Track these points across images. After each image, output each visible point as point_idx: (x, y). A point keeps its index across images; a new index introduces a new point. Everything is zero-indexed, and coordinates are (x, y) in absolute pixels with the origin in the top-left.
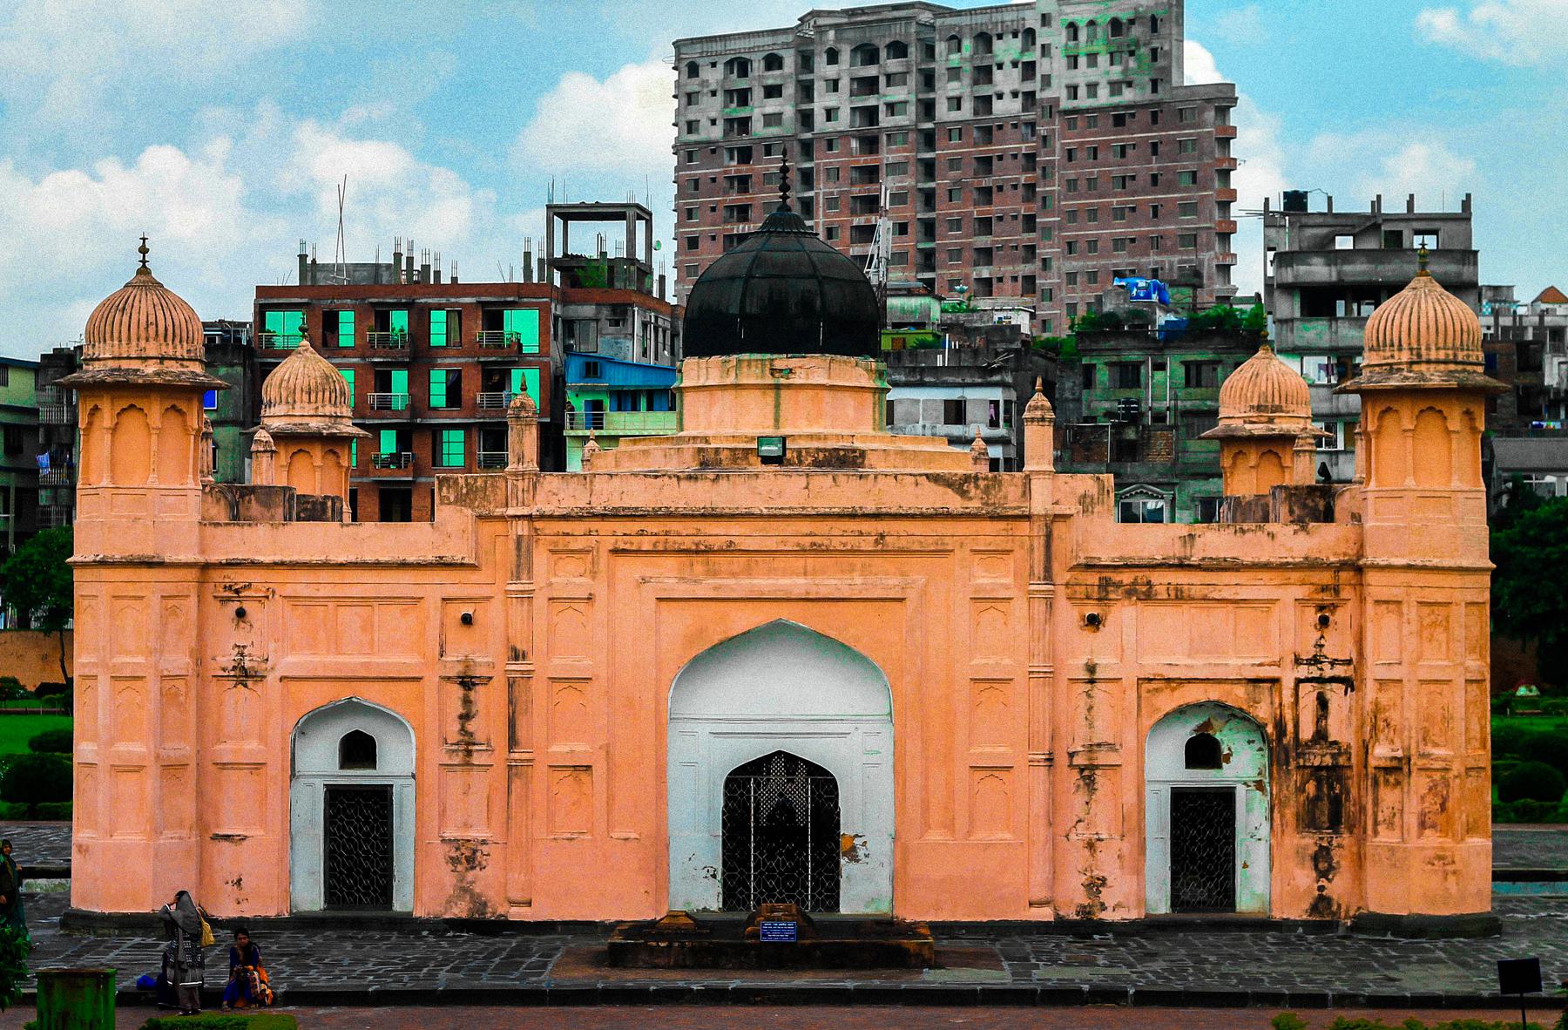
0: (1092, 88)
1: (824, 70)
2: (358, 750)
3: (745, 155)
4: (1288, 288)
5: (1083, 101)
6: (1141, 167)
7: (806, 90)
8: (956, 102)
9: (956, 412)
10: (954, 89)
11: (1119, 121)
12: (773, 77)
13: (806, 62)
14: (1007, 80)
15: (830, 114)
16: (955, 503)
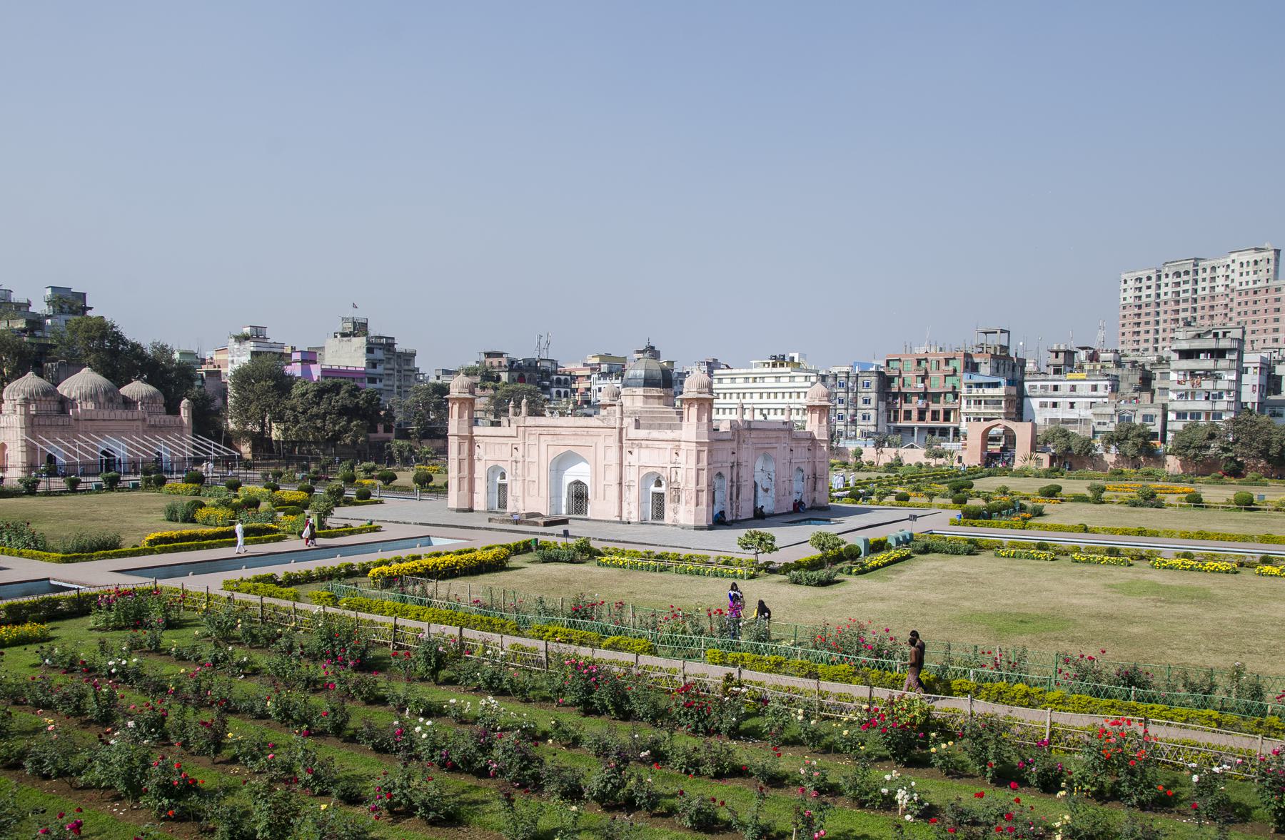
0: (1247, 283)
1: (1164, 280)
2: (503, 476)
3: (1140, 307)
4: (1175, 351)
5: (1244, 287)
6: (1251, 307)
7: (1159, 287)
8: (1204, 289)
9: (1095, 388)
10: (1204, 284)
11: (1255, 293)
12: (1149, 283)
13: (1159, 278)
14: (1220, 281)
15: (1166, 294)
16: (601, 424)
